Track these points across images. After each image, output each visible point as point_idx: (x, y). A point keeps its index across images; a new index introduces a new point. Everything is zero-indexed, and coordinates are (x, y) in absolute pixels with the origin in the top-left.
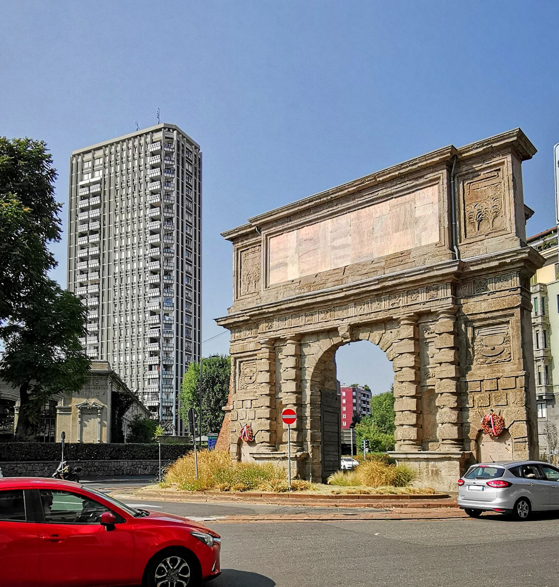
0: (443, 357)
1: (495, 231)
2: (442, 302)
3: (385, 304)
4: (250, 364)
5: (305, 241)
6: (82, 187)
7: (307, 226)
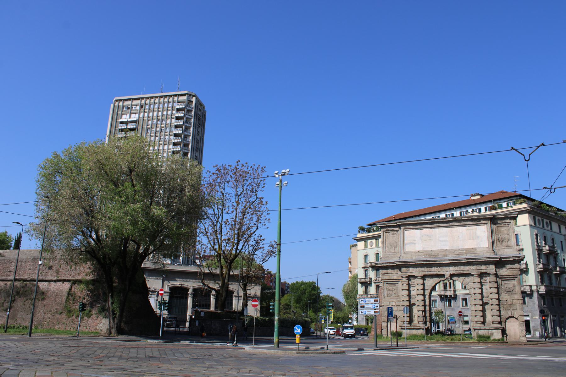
1: (509, 246)
2: (491, 270)
6: (121, 123)
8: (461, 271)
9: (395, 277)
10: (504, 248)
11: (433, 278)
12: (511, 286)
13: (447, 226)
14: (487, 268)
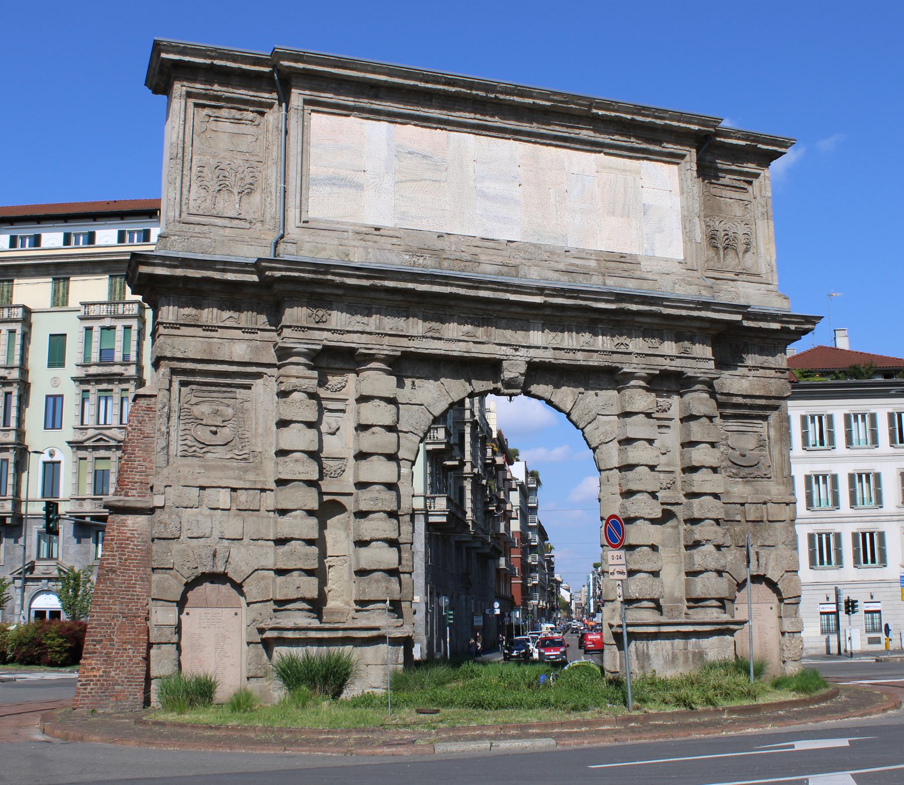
0: (705, 457)
1: (753, 275)
3: (603, 342)
4: (215, 395)
5: (410, 153)
7: (416, 125)
8: (580, 356)
9: (240, 351)
10: (731, 276)
11: (436, 379)
12: (748, 443)
13: (516, 134)
14: (686, 352)
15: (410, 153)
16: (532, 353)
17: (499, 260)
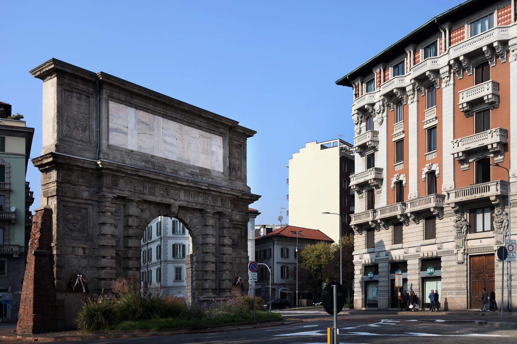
5: (142, 122)
15: (142, 122)
16: (181, 202)
17: (171, 168)
